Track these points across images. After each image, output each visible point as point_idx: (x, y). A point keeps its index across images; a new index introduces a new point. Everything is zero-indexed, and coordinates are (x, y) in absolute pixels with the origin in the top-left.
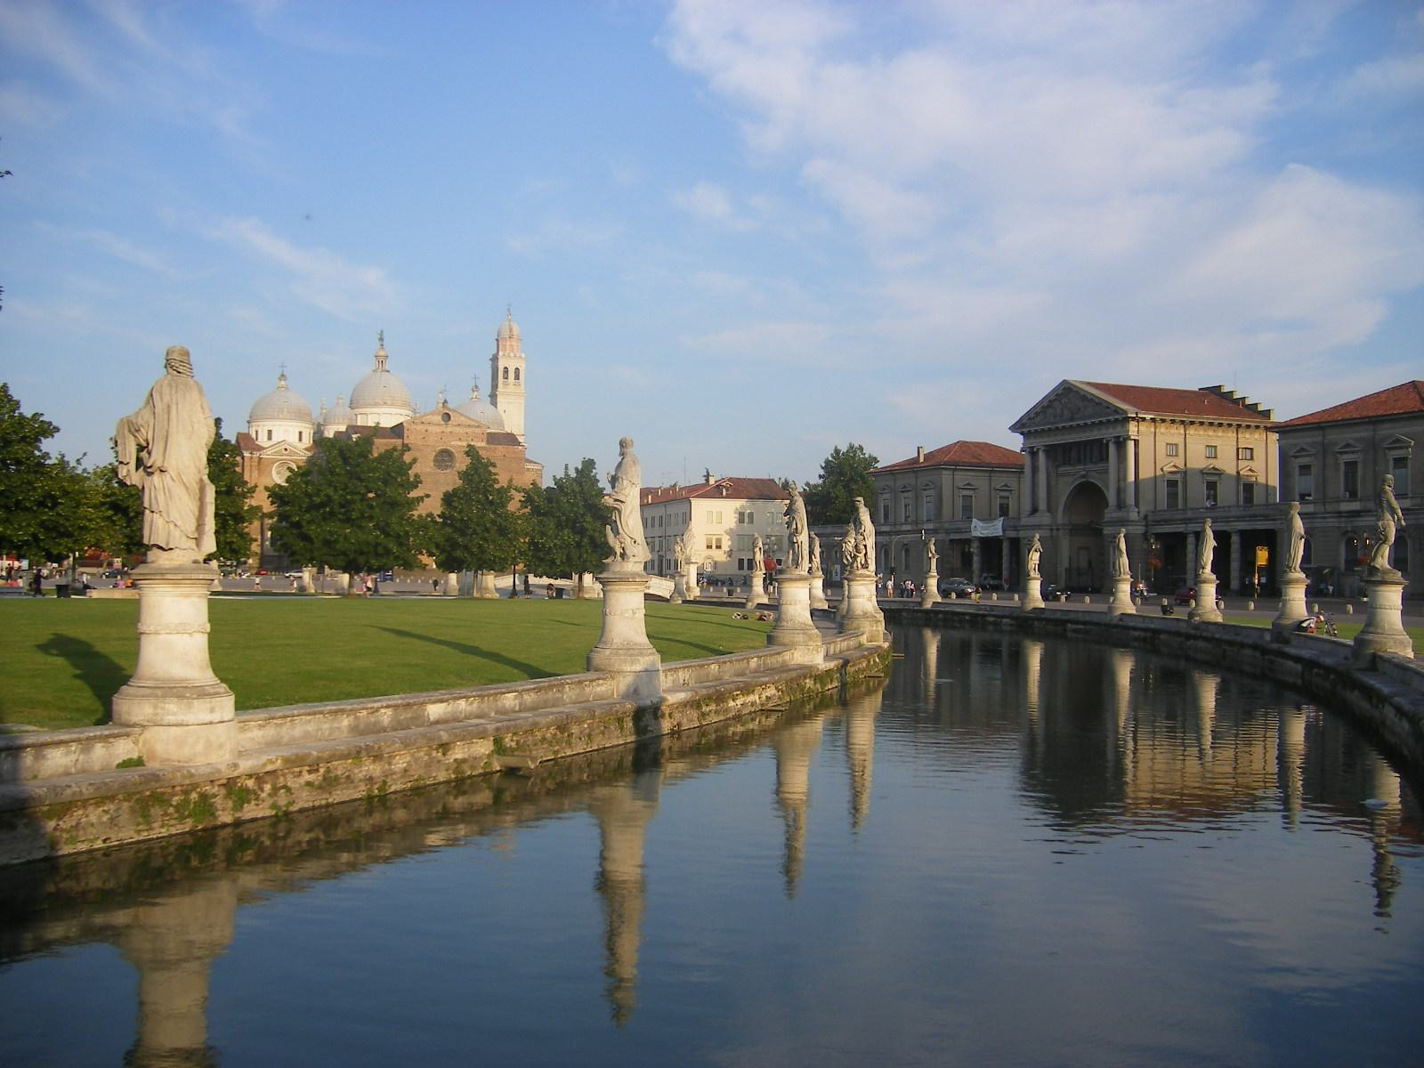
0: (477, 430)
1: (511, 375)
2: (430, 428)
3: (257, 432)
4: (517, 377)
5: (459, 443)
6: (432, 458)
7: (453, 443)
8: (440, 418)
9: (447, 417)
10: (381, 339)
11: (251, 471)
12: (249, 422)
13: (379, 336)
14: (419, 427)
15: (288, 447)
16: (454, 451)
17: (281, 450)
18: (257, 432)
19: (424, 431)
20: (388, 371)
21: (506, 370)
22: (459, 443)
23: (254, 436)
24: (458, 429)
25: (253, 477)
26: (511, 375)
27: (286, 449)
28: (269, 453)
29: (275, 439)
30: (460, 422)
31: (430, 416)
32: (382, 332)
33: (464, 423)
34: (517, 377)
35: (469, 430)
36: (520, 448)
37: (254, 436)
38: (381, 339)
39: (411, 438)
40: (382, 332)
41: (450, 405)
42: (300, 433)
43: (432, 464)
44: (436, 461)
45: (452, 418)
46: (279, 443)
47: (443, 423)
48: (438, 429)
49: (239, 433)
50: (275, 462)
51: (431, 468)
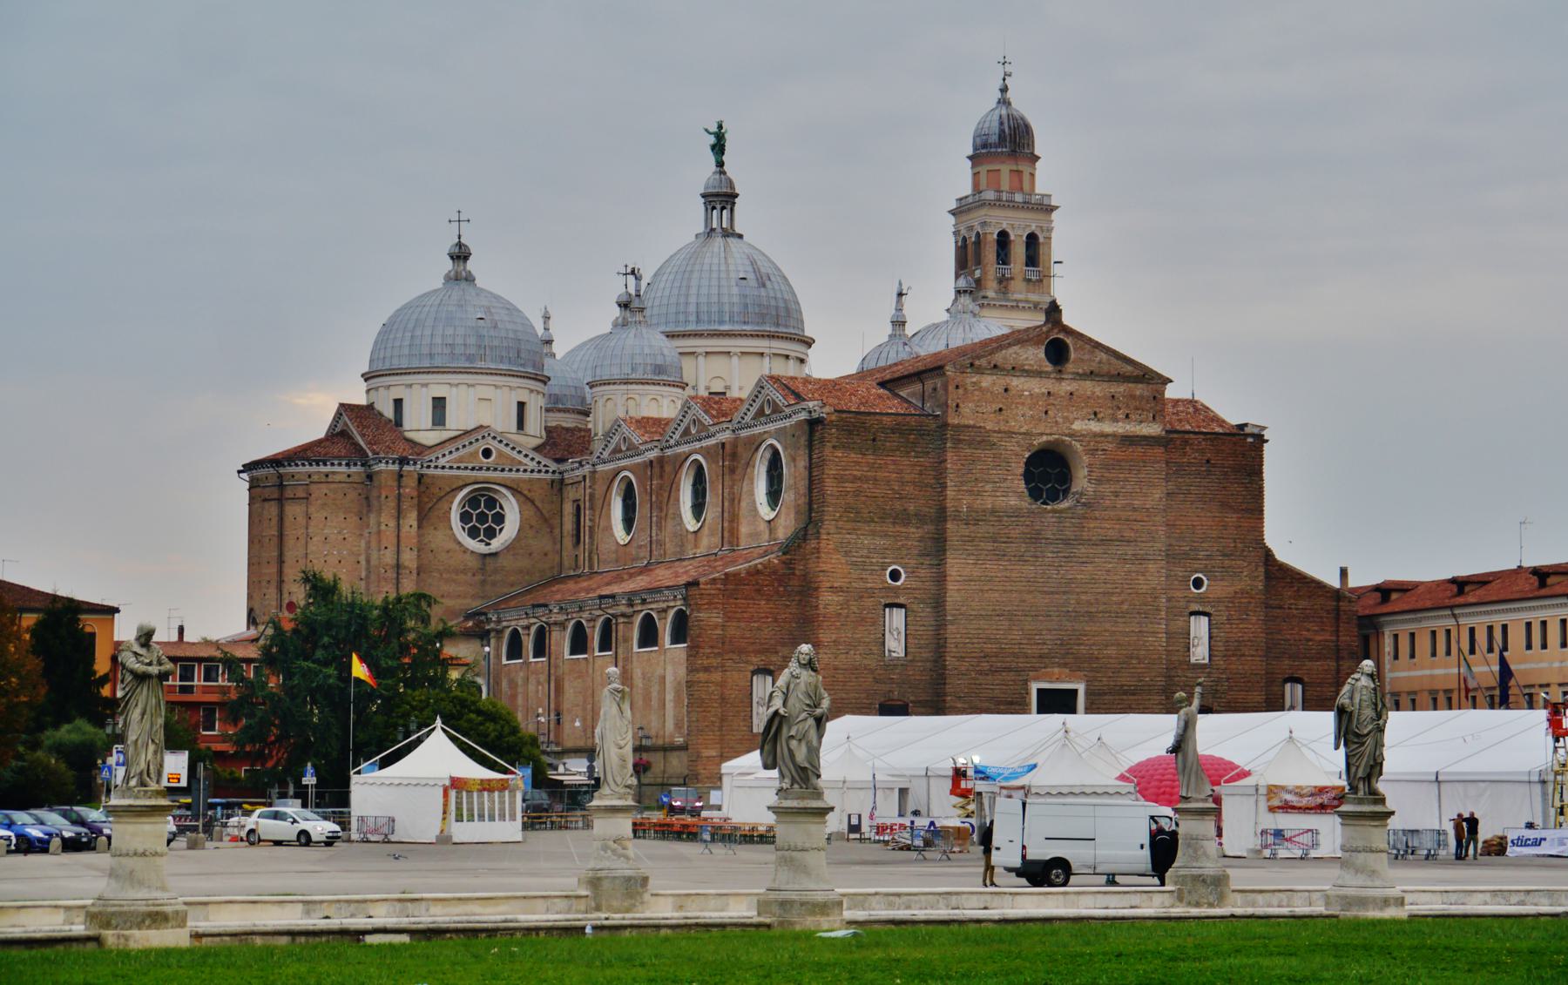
0: (1140, 389)
1: (1018, 251)
2: (1016, 382)
3: (398, 403)
4: (1032, 260)
5: (1095, 427)
6: (1021, 471)
7: (1077, 426)
8: (1042, 355)
9: (1057, 352)
10: (719, 148)
11: (399, 515)
12: (367, 377)
13: (712, 140)
14: (987, 381)
15: (493, 445)
16: (1077, 446)
17: (474, 455)
18: (398, 403)
19: (999, 389)
20: (740, 236)
21: (1003, 239)
22: (1095, 427)
23: (389, 413)
24: (1089, 387)
25: (405, 529)
26: (1018, 251)
27: (487, 453)
28: (442, 462)
29: (458, 420)
30: (1094, 366)
31: (1011, 350)
32: (720, 127)
33: (1105, 368)
34: (1032, 260)
35: (1120, 389)
36: (1250, 440)
37: (389, 413)
38: (719, 148)
39: (967, 409)
40: (720, 127)
41: (1067, 319)
42: (521, 405)
43: (1022, 484)
44: (1028, 476)
45: (1073, 356)
46: (467, 433)
47: (1049, 367)
48: (1036, 386)
49: (342, 405)
50: (461, 488)
51: (1020, 495)
